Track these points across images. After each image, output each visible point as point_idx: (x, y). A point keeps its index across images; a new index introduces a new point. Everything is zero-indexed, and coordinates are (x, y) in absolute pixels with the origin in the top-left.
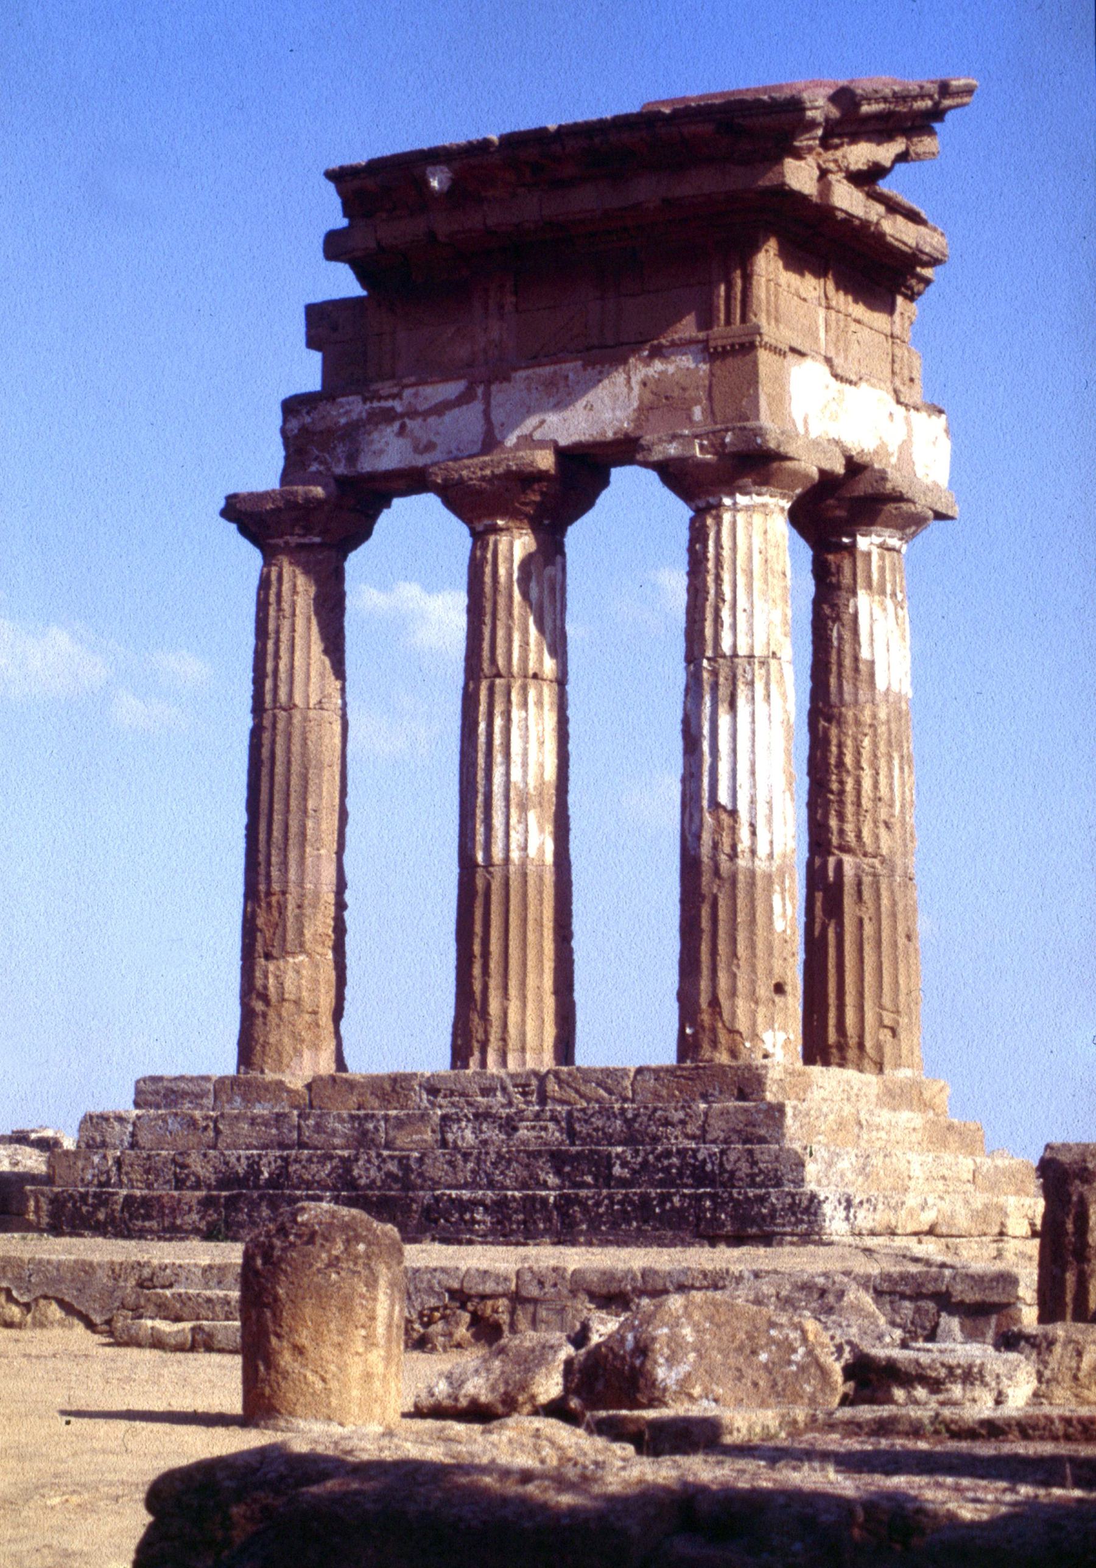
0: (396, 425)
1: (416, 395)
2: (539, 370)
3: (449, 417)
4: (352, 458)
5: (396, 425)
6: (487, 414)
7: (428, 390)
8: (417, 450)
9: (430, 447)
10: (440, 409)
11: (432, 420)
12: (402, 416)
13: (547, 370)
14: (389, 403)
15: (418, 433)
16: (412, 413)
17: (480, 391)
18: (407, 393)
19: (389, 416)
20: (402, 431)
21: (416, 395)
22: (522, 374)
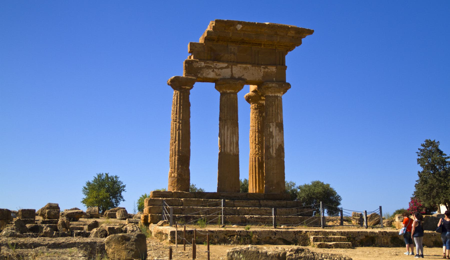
0: (212, 70)
1: (216, 65)
2: (243, 65)
3: (223, 70)
4: (202, 74)
5: (212, 70)
6: (232, 71)
7: (218, 64)
8: (216, 75)
9: (219, 75)
10: (222, 68)
11: (220, 70)
12: (213, 68)
13: (244, 66)
14: (210, 65)
15: (217, 72)
16: (216, 68)
17: (230, 67)
18: (215, 64)
19: (209, 67)
20: (213, 71)
21: (216, 65)
22: (239, 65)
